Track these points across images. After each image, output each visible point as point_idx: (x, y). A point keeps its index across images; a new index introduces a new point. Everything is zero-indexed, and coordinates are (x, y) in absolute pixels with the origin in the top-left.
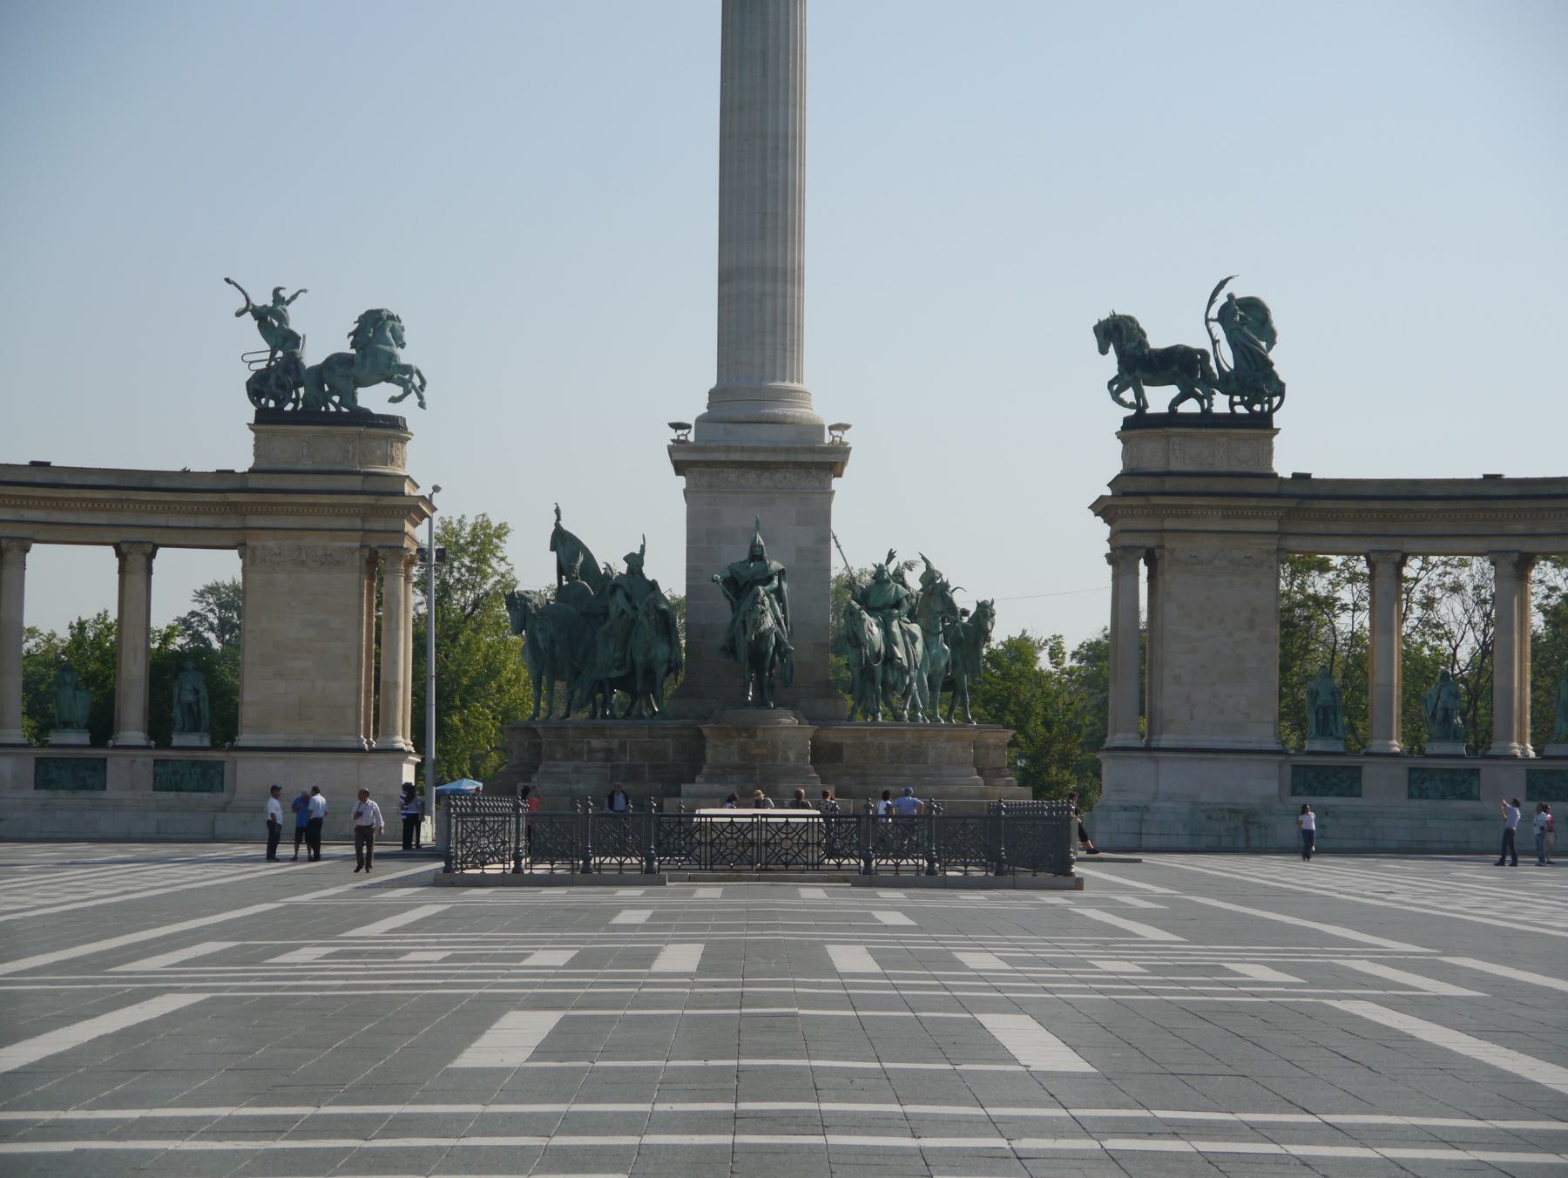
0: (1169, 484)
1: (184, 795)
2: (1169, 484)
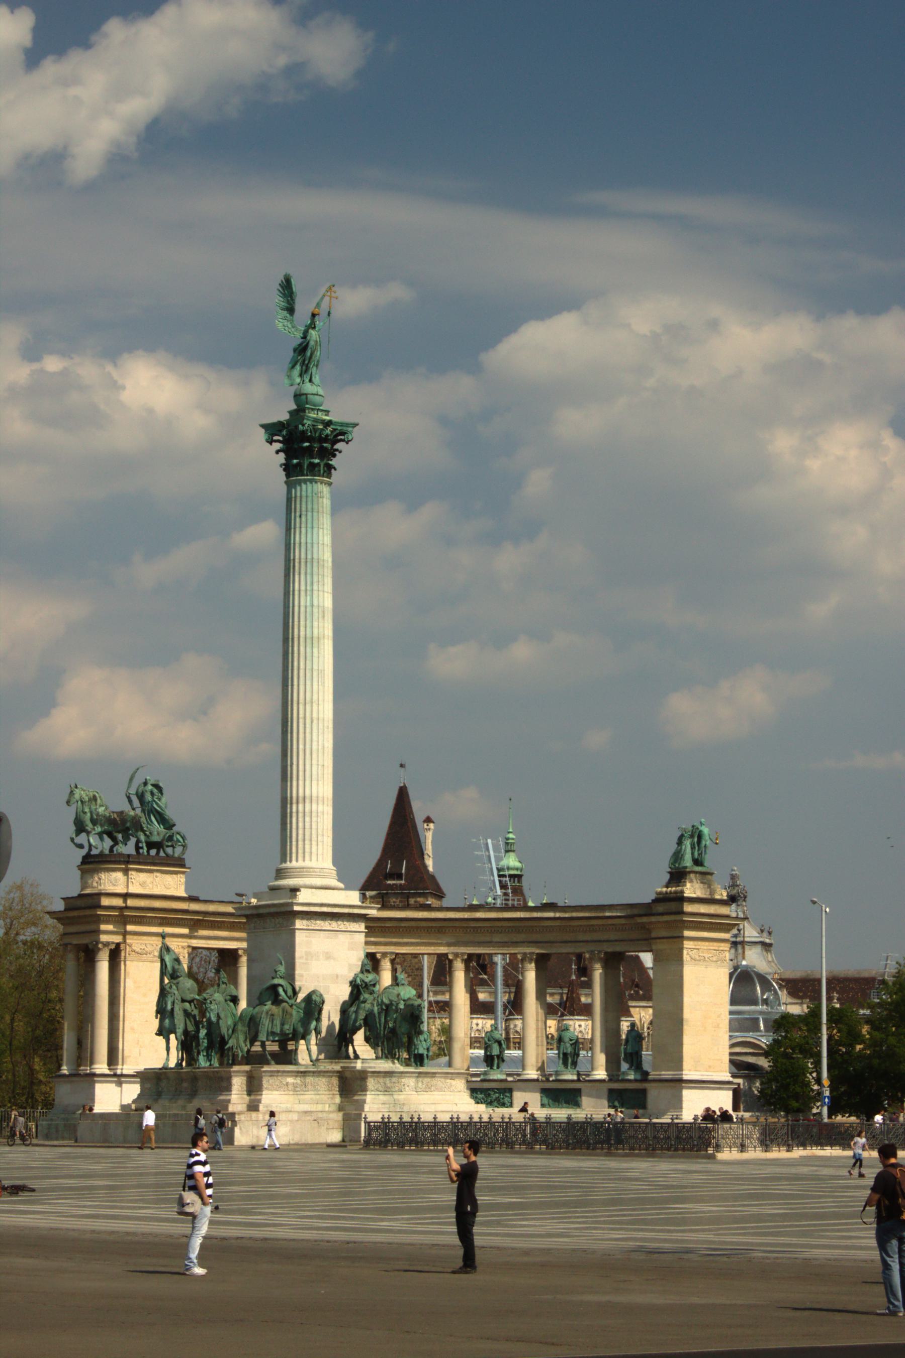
0: (131, 902)
2: (131, 902)
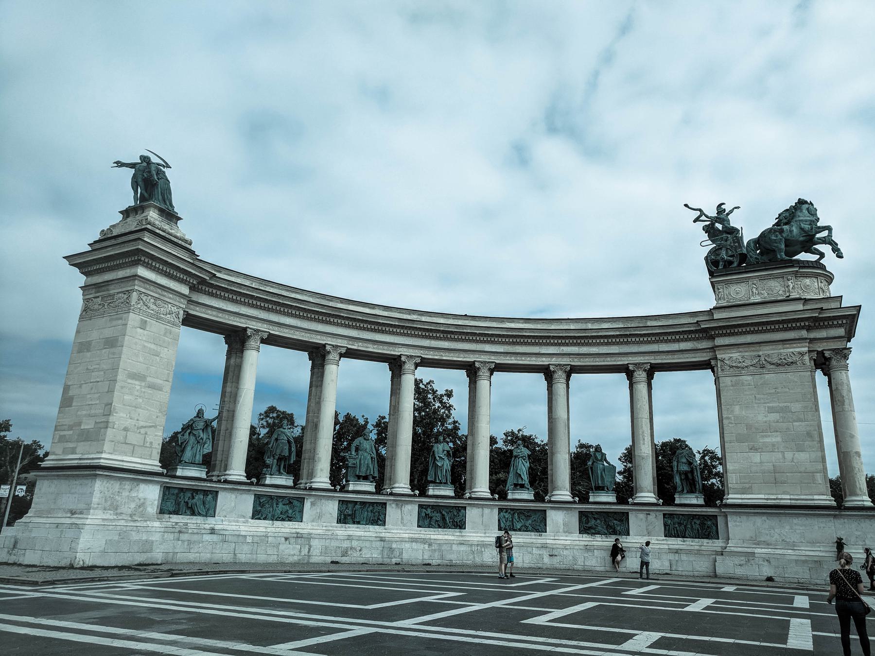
1: (689, 541)
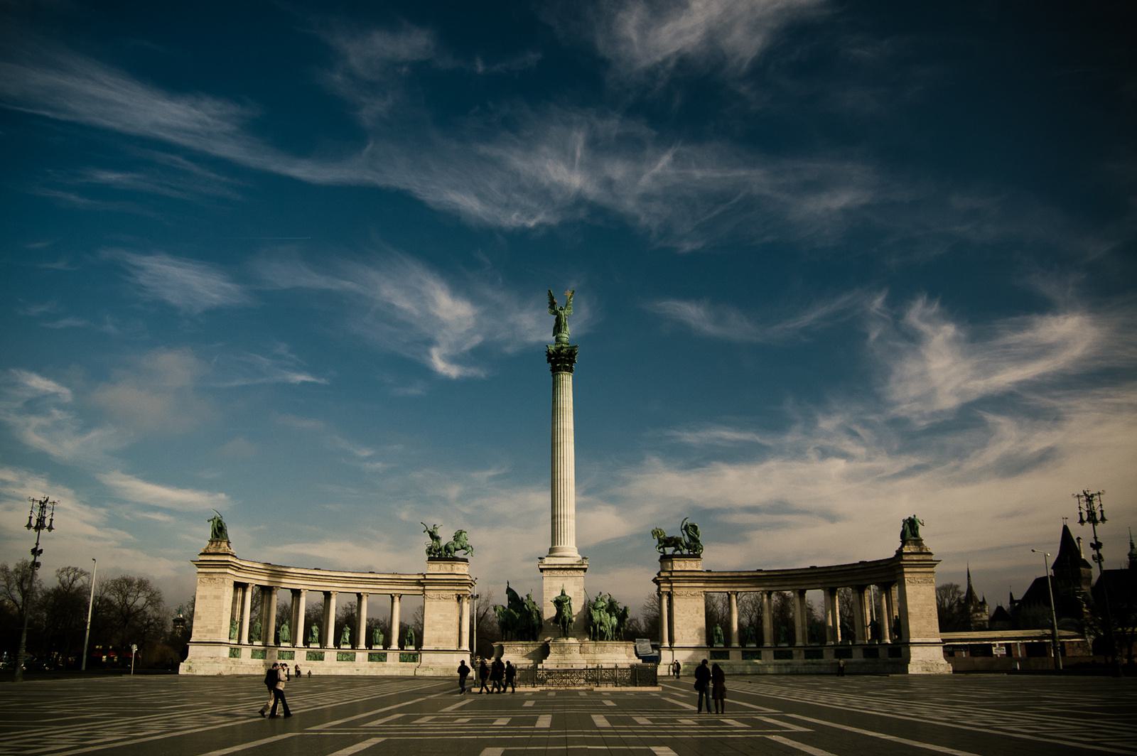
2: (673, 574)
